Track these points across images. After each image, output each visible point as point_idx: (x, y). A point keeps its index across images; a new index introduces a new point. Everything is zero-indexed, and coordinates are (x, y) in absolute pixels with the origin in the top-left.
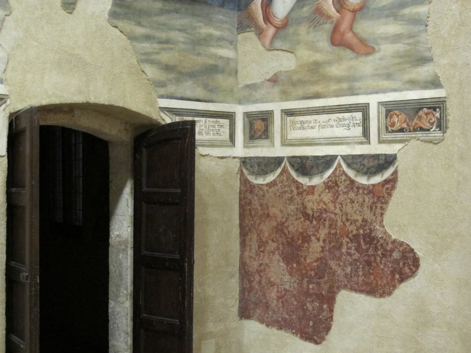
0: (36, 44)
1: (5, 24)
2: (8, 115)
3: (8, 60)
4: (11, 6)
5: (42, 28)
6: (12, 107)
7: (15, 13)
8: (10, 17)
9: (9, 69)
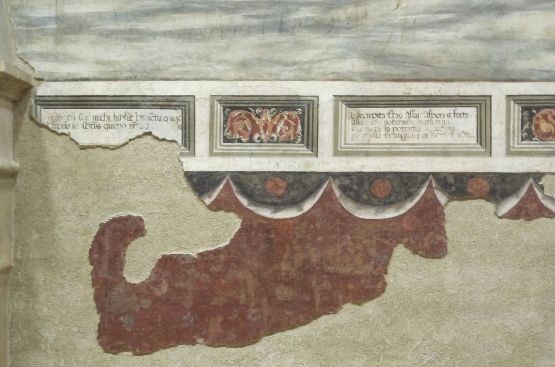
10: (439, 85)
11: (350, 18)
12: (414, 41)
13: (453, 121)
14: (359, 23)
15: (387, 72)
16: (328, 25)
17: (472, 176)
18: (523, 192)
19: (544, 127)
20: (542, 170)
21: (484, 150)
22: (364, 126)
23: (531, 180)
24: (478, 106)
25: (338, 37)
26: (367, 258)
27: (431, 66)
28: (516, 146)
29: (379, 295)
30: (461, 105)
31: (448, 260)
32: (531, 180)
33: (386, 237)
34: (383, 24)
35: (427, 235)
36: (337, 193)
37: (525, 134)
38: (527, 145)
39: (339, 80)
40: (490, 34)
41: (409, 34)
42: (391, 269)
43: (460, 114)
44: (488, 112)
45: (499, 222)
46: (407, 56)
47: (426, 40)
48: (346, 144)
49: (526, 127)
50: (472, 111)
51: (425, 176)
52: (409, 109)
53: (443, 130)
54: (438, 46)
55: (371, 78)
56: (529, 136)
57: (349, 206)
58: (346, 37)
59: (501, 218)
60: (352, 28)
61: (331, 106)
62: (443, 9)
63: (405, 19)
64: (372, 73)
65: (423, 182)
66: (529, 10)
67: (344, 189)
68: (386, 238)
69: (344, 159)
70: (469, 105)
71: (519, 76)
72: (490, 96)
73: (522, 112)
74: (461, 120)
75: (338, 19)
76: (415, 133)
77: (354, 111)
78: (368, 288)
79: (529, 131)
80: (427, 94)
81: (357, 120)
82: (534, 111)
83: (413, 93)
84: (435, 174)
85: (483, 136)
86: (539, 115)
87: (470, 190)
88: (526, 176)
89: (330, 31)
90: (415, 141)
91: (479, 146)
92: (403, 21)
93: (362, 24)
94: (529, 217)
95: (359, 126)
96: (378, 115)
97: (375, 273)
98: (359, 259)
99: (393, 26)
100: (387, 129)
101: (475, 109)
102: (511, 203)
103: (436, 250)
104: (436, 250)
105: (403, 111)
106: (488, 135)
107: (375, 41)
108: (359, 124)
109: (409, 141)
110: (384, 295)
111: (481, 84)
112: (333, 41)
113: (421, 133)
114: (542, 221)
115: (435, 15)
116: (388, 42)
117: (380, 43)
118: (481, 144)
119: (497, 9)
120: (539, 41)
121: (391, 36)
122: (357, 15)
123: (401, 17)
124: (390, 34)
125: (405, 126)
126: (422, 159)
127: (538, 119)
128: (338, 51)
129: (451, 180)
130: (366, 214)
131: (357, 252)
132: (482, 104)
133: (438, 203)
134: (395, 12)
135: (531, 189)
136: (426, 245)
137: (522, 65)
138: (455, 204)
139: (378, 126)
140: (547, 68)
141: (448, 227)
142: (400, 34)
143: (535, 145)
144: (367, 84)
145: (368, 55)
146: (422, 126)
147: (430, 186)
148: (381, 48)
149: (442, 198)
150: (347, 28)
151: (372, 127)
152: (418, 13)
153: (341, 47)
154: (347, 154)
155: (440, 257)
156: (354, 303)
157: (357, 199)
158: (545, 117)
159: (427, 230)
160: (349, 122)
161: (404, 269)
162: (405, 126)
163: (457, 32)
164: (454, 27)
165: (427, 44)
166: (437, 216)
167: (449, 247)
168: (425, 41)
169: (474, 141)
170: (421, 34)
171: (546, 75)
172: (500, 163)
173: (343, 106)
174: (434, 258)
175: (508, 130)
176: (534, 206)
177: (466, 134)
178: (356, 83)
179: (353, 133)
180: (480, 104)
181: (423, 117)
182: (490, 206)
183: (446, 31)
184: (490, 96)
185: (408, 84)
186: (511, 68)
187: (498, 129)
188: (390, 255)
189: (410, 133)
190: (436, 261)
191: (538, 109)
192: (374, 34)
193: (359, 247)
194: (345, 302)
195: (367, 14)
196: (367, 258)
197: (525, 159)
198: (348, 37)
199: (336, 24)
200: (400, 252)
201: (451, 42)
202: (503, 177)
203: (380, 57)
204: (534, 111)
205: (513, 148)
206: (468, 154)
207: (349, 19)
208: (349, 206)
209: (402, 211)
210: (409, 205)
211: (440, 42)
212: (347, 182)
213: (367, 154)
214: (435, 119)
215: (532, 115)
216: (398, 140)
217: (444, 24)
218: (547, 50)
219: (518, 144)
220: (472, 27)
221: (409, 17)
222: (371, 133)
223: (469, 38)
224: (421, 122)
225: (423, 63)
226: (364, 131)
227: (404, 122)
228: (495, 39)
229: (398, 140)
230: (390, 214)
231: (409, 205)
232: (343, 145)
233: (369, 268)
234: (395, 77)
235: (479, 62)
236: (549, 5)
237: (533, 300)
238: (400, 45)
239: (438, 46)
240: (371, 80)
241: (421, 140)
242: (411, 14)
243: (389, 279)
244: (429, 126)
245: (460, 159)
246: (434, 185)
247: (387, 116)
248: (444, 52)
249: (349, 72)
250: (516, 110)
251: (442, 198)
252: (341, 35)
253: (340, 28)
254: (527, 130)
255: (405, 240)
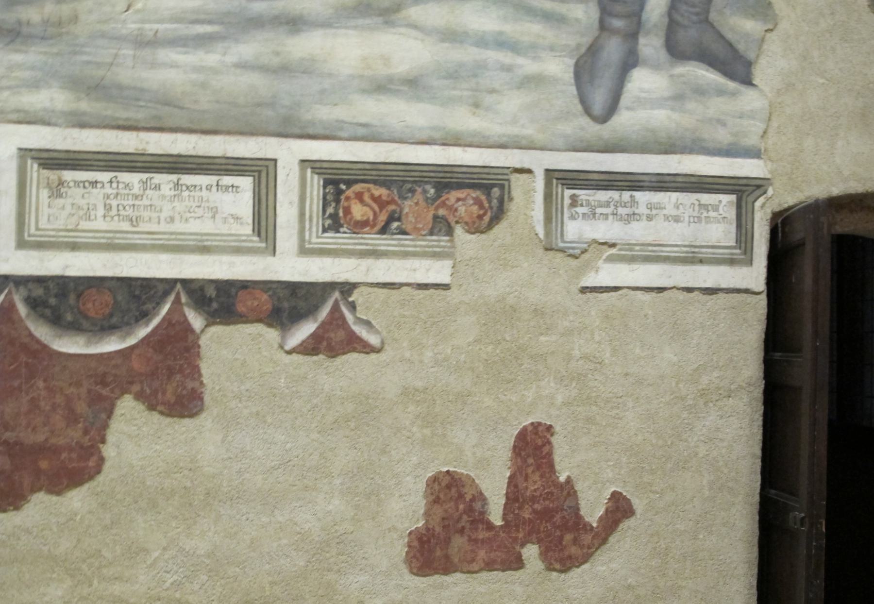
0: (821, 81)
1: (765, 47)
2: (769, 216)
3: (770, 114)
4: (777, 12)
5: (833, 50)
6: (777, 201)
7: (784, 25)
8: (774, 33)
9: (771, 132)
10: (193, 138)
11: (48, 21)
12: (154, 65)
13: (216, 197)
14: (64, 30)
15: (109, 113)
16: (10, 31)
17: (245, 285)
18: (324, 313)
19: (358, 211)
20: (353, 280)
21: (263, 245)
22: (69, 201)
23: (337, 295)
24: (256, 174)
25: (26, 52)
26: (72, 418)
27: (182, 108)
28: (314, 240)
29: (91, 478)
30: (229, 172)
31: (205, 420)
32: (337, 295)
33: (104, 383)
34: (103, 35)
35: (171, 381)
36: (22, 309)
37: (328, 222)
38: (331, 239)
39: (29, 123)
40: (276, 61)
41: (146, 53)
42: (111, 437)
43: (227, 187)
44: (271, 184)
45: (287, 359)
46: (142, 90)
47: (174, 65)
48: (37, 229)
49: (330, 210)
50: (246, 183)
51: (170, 284)
52: (144, 176)
53: (200, 212)
54: (194, 76)
55: (81, 122)
56: (334, 224)
57: (42, 332)
58: (41, 53)
59: (289, 353)
60: (51, 38)
61: (14, 165)
62: (202, 17)
63: (139, 29)
64: (84, 114)
65: (166, 294)
66: (337, 28)
67: (34, 304)
68: (104, 383)
69: (34, 253)
70: (241, 173)
71: (321, 131)
72: (275, 161)
73: (325, 187)
74: (228, 197)
75: (28, 23)
76: (154, 215)
77: (53, 175)
78: (75, 466)
79: (334, 217)
80: (175, 152)
81: (57, 190)
82: (343, 187)
83: (151, 150)
84: (185, 282)
85: (263, 223)
86: (350, 193)
87: (241, 308)
88: (331, 286)
89: (12, 41)
90: (154, 228)
91: (256, 238)
92: (135, 32)
93: (67, 33)
94: (333, 352)
95: (61, 201)
96: (94, 184)
97: (86, 441)
98: (58, 420)
99: (120, 39)
100: (108, 208)
101: (251, 179)
102: (305, 330)
103: (185, 403)
104: (185, 403)
105: (134, 179)
106: (271, 221)
107: (88, 63)
108: (60, 196)
109: (144, 227)
110: (100, 478)
111: (261, 139)
112: (17, 58)
113: (163, 215)
114: (353, 357)
115: (190, 26)
116: (111, 64)
117: (99, 65)
118: (259, 235)
119: (287, 23)
120: (352, 77)
121: (116, 55)
122: (60, 18)
123: (133, 26)
124: (114, 51)
125: (137, 202)
126: (165, 257)
127: (348, 199)
128: (27, 74)
129: (211, 292)
130: (71, 345)
131: (54, 407)
132: (262, 172)
133: (189, 329)
134: (123, 16)
135: (336, 308)
136: (170, 396)
137: (325, 113)
138: (217, 330)
139: (92, 201)
140: (363, 120)
141: (206, 369)
142: (131, 52)
143: (342, 239)
144: (75, 132)
145: (78, 85)
146: (166, 204)
147: (177, 300)
148: (101, 73)
149: (196, 320)
150: (43, 38)
151: (83, 202)
152: (161, 21)
153: (33, 68)
154: (40, 246)
155: (192, 416)
156: (50, 492)
157: (56, 321)
158: (359, 196)
159: (171, 372)
160: (44, 193)
161: (134, 434)
162: (137, 202)
163: (224, 54)
164: (220, 46)
165: (174, 71)
166: (187, 349)
167: (207, 398)
168: (172, 67)
169: (248, 230)
170: (167, 55)
171: (361, 131)
172: (288, 266)
173: (33, 168)
174: (182, 416)
175: (302, 214)
176: (341, 334)
177: (237, 218)
178: (57, 130)
179: (51, 211)
180: (260, 172)
181: (167, 190)
182: (272, 334)
183: (207, 53)
184: (275, 161)
185: (143, 135)
186: (308, 117)
187: (286, 213)
188: (110, 414)
189: (146, 214)
190: (186, 421)
191: (349, 183)
192: (87, 50)
193: (59, 399)
194: (34, 490)
195: (76, 17)
196: (72, 418)
197: (327, 261)
198: (45, 53)
199: (25, 30)
200: (128, 408)
201: (214, 71)
202: (293, 288)
203: (97, 89)
204: (343, 187)
205: (310, 243)
206: (238, 251)
207: (46, 22)
208: (42, 332)
209: (131, 341)
210: (143, 332)
211: (197, 69)
212: (38, 292)
213: (74, 247)
214: (186, 194)
215: (339, 192)
216: (126, 226)
217: (203, 41)
218: (364, 91)
219: (318, 237)
220: (249, 48)
221: (147, 26)
222: (81, 213)
223: (243, 66)
224: (164, 197)
225: (167, 103)
226: (68, 208)
227: (136, 197)
228: (284, 70)
229: (126, 226)
230: (111, 345)
231: (143, 332)
232: (33, 231)
233: (75, 434)
234: (121, 123)
235: (259, 105)
236: (368, 21)
237: (338, 481)
238: (130, 71)
239: (194, 76)
240: (82, 125)
241: (163, 227)
242: (150, 22)
243: (109, 451)
244: (176, 204)
245: (226, 258)
246: (184, 299)
247: (107, 185)
248: (204, 85)
249: (45, 110)
250: (315, 184)
251: (196, 320)
252: (33, 48)
253: (30, 36)
254: (331, 216)
255: (136, 388)
